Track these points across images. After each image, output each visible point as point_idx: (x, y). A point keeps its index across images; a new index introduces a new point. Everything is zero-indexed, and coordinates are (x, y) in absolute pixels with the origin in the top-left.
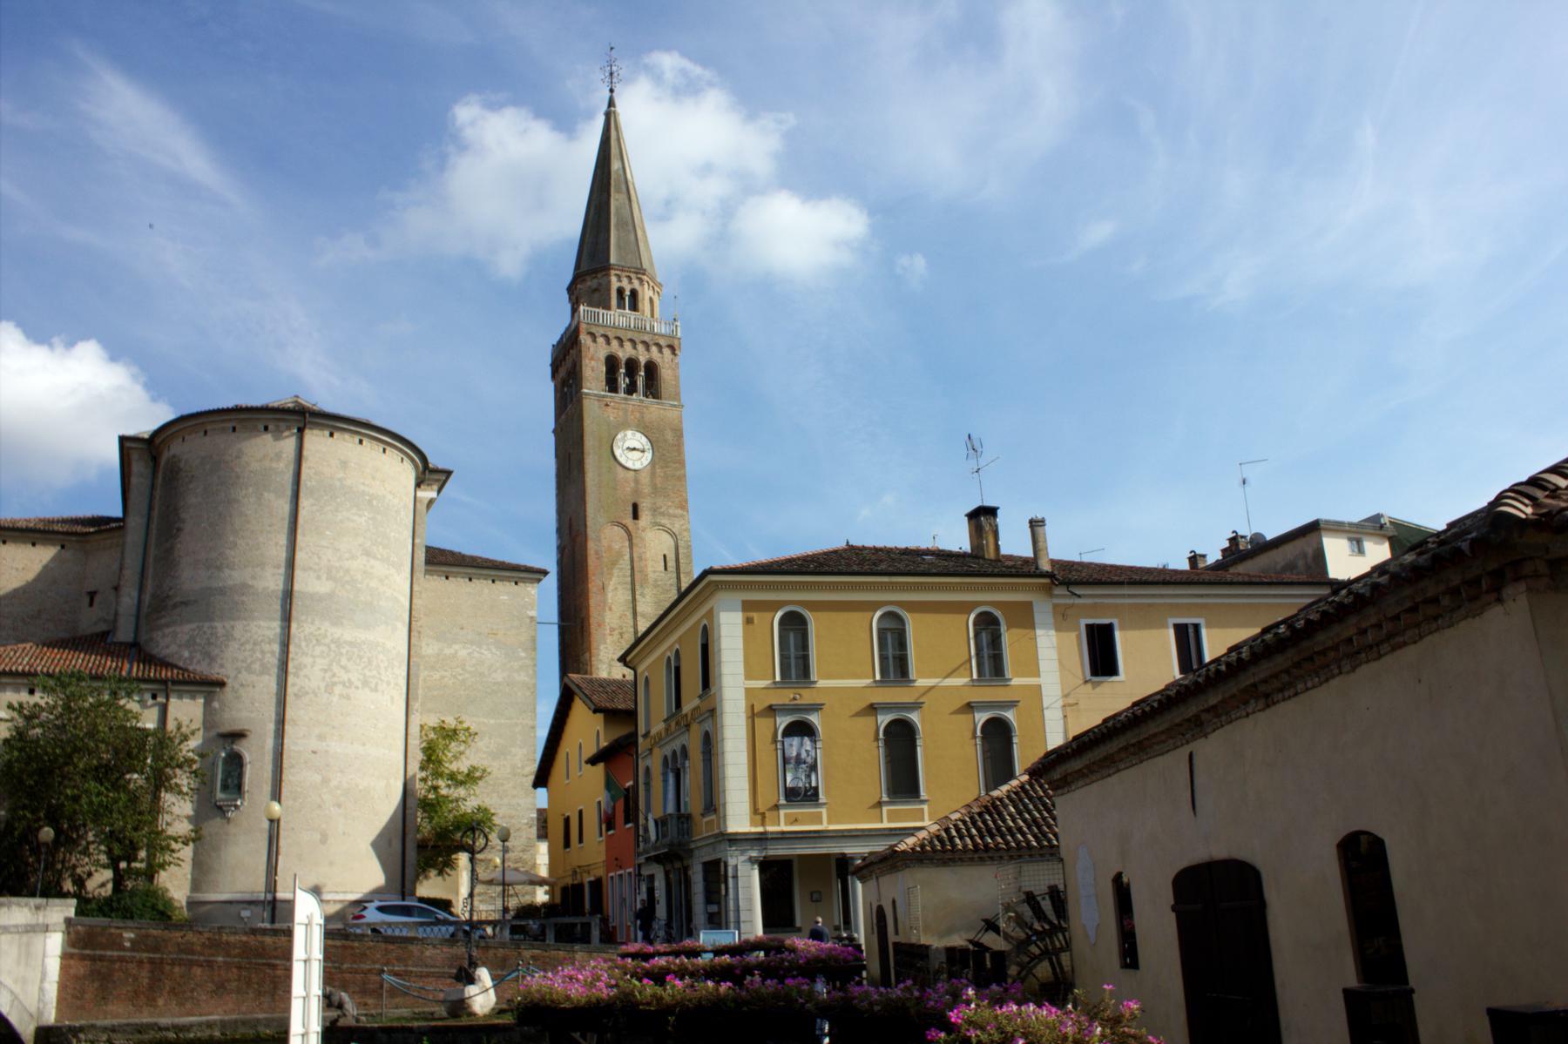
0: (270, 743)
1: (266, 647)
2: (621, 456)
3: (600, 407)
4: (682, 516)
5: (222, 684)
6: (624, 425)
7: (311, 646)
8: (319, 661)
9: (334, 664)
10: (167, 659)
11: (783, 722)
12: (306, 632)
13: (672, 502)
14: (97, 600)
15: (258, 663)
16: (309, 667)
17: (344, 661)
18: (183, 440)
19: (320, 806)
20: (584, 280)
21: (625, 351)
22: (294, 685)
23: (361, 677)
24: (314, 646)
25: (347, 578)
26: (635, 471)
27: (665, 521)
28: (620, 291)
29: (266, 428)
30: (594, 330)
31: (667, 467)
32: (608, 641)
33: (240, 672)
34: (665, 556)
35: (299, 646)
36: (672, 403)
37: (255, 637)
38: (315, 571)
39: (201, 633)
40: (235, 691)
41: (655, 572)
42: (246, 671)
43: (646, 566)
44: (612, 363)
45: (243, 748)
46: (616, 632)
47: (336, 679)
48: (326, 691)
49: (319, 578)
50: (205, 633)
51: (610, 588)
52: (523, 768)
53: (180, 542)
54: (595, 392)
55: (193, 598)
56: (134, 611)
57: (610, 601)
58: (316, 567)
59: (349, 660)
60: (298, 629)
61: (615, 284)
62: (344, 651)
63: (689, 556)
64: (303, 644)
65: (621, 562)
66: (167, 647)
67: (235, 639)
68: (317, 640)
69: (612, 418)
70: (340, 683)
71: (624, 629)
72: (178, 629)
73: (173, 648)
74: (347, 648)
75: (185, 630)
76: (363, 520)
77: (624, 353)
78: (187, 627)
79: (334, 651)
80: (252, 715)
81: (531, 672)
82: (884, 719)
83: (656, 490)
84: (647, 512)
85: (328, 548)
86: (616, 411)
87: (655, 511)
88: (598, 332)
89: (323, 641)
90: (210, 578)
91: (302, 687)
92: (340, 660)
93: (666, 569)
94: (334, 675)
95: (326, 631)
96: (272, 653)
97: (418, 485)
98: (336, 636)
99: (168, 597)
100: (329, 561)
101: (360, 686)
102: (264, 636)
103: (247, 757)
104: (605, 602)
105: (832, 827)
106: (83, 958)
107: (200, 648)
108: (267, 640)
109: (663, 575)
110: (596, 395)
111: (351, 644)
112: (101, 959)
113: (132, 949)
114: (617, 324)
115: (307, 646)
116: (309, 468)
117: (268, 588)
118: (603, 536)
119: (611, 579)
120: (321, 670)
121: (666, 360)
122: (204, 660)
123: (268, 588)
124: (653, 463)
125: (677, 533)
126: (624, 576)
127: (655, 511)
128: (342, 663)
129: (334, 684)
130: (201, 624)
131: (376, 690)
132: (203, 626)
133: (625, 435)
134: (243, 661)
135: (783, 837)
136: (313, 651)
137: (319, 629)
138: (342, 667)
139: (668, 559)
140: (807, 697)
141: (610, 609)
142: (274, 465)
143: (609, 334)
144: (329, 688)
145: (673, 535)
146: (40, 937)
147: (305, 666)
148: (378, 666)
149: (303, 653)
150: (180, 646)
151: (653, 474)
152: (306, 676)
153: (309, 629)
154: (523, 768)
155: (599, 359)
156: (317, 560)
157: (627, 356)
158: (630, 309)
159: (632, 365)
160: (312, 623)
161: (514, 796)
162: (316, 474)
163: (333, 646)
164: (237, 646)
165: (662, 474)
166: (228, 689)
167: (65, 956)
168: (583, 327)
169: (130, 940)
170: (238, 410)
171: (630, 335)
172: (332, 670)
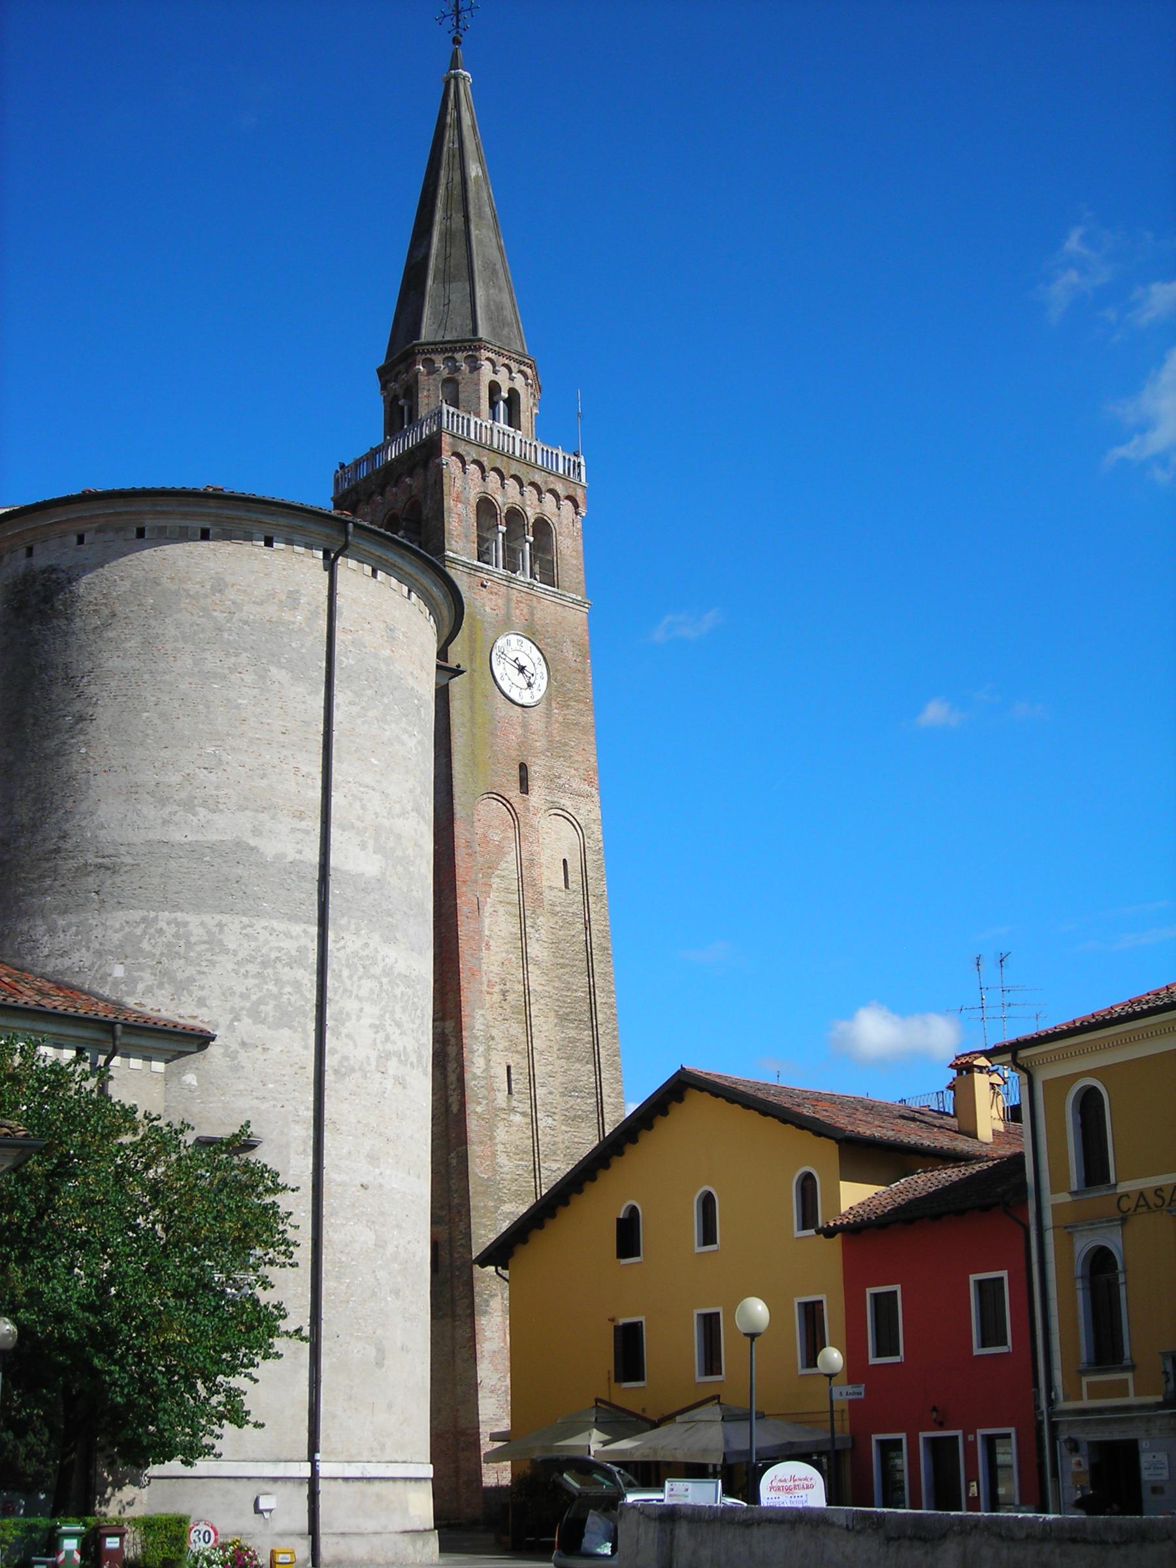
1: (286, 973)
5: (201, 1040)
6: (506, 625)
7: (355, 978)
8: (368, 1008)
9: (387, 1015)
12: (348, 950)
15: (272, 1003)
16: (354, 1017)
22: (334, 1051)
24: (360, 978)
25: (399, 853)
26: (523, 706)
27: (566, 802)
28: (494, 388)
29: (141, 533)
33: (237, 1018)
35: (339, 976)
36: (574, 596)
39: (152, 931)
40: (232, 1056)
42: (249, 1016)
44: (485, 507)
47: (389, 1047)
49: (363, 846)
50: (161, 931)
51: (487, 909)
53: (87, 744)
54: (464, 558)
57: (487, 933)
58: (358, 824)
59: (404, 1009)
62: (398, 992)
64: (346, 973)
66: (64, 954)
67: (227, 952)
68: (364, 967)
69: (487, 609)
76: (412, 743)
77: (506, 496)
80: (264, 1106)
84: (540, 783)
86: (494, 597)
88: (469, 454)
89: (372, 971)
90: (165, 822)
91: (346, 1058)
92: (393, 1012)
93: (567, 887)
94: (387, 1039)
96: (297, 985)
100: (376, 813)
102: (280, 949)
104: (479, 932)
117: (284, 856)
121: (565, 522)
122: (161, 986)
124: (548, 697)
126: (507, 890)
127: (552, 780)
128: (397, 1016)
129: (388, 1055)
130: (152, 914)
133: (508, 643)
134: (242, 996)
136: (359, 987)
138: (399, 1025)
141: (488, 949)
142: (287, 616)
143: (485, 461)
149: (345, 991)
150: (99, 954)
151: (548, 714)
152: (348, 1036)
156: (361, 812)
159: (515, 516)
160: (357, 933)
163: (385, 980)
164: (230, 966)
165: (561, 719)
170: (87, 497)
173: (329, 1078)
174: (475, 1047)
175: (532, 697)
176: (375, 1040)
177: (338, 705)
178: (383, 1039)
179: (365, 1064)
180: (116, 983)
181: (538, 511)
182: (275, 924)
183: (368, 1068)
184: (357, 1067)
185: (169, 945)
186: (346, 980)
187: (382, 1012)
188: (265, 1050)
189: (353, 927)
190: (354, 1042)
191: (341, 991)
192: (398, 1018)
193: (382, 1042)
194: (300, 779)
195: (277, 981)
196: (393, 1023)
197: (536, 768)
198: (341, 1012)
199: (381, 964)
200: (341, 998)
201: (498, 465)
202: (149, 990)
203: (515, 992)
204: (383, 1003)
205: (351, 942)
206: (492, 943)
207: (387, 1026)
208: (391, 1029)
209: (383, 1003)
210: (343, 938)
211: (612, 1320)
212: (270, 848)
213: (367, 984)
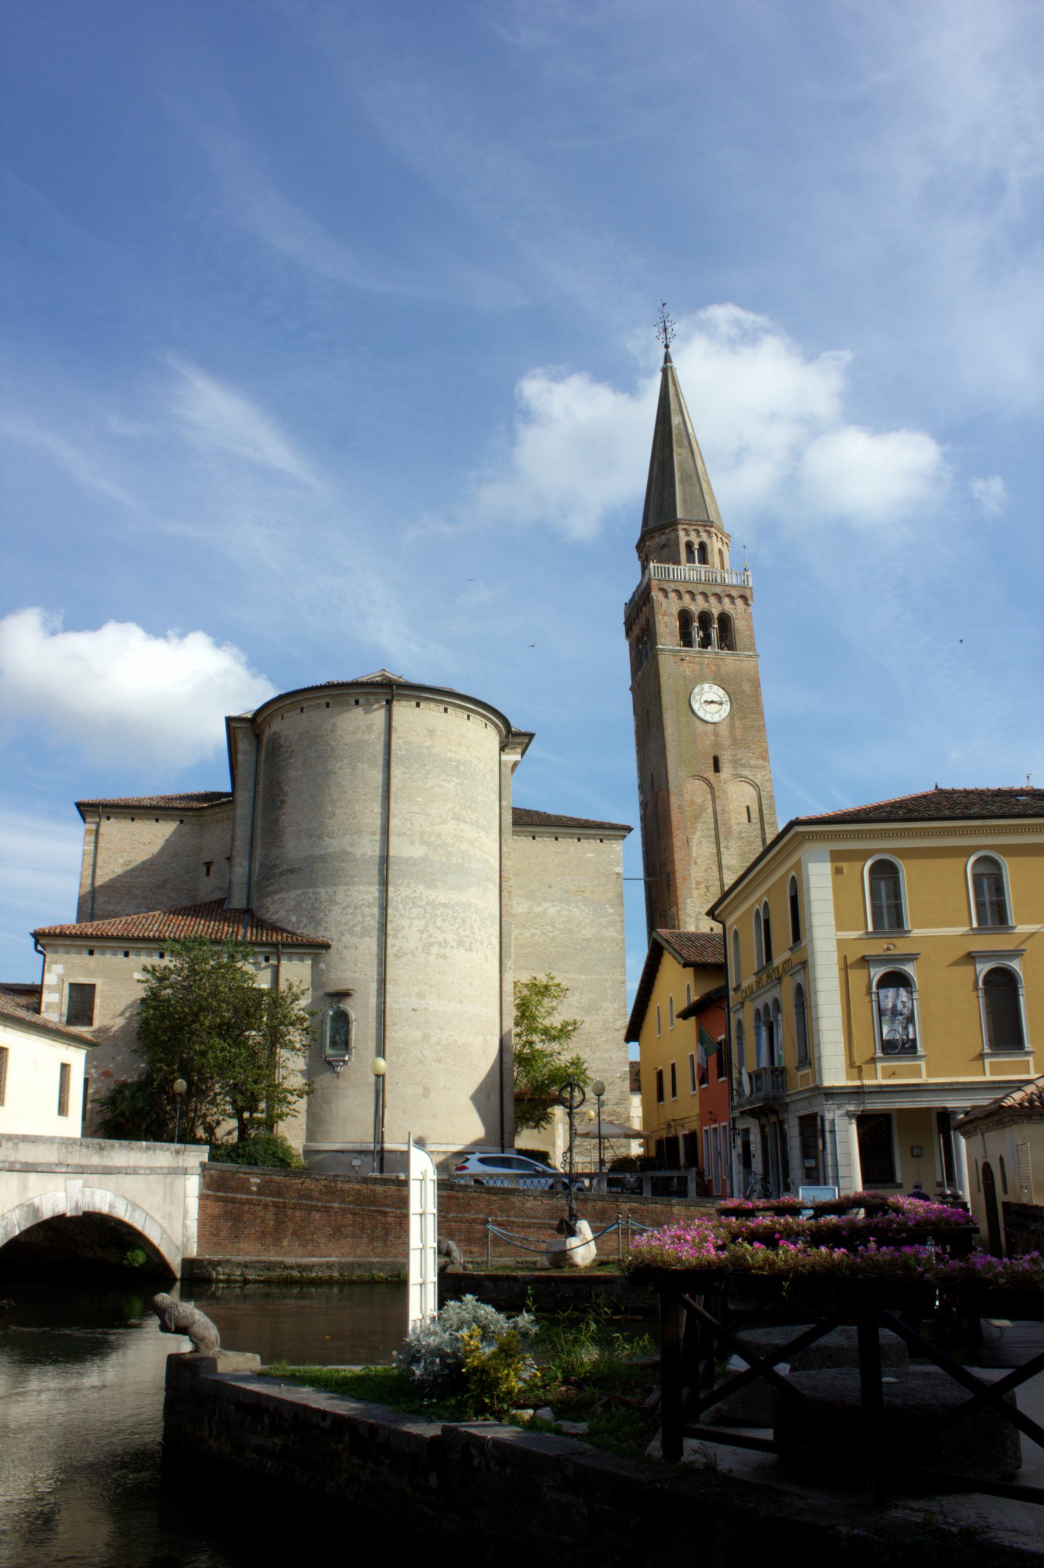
0: (373, 1001)
1: (367, 911)
2: (699, 710)
3: (676, 663)
4: (763, 767)
5: (327, 946)
6: (701, 679)
7: (407, 908)
8: (415, 922)
9: (430, 925)
10: (277, 924)
11: (877, 973)
12: (402, 896)
13: (753, 753)
14: (213, 869)
17: (439, 923)
18: (282, 719)
19: (421, 1062)
20: (653, 537)
21: (697, 605)
22: (393, 946)
23: (456, 937)
24: (410, 908)
25: (439, 842)
26: (714, 723)
27: (745, 773)
28: (689, 545)
30: (665, 586)
31: (746, 718)
32: (695, 895)
33: (343, 935)
34: (748, 808)
35: (396, 909)
36: (747, 653)
37: (356, 901)
38: (408, 837)
41: (738, 824)
43: (729, 818)
44: (685, 617)
45: (347, 1006)
46: (702, 885)
47: (432, 940)
48: (423, 951)
49: (412, 843)
50: (310, 898)
51: (695, 842)
52: (614, 1022)
54: (670, 647)
55: (297, 866)
56: (245, 880)
57: (695, 855)
58: (409, 833)
59: (444, 921)
60: (395, 892)
61: (683, 539)
62: (439, 912)
63: (772, 807)
64: (401, 907)
65: (704, 815)
66: (277, 912)
67: (338, 904)
68: (413, 903)
69: (688, 673)
70: (436, 943)
71: (710, 882)
72: (286, 895)
73: (282, 914)
74: (442, 910)
75: (291, 897)
76: (451, 785)
77: (696, 607)
78: (293, 894)
79: (430, 913)
80: (356, 975)
81: (619, 928)
82: (983, 968)
83: (735, 742)
85: (419, 813)
87: (736, 762)
88: (669, 587)
89: (418, 903)
90: (312, 846)
91: (401, 948)
92: (435, 922)
93: (749, 821)
94: (430, 936)
95: (421, 893)
96: (372, 915)
97: (502, 749)
98: (431, 898)
99: (275, 865)
100: (421, 826)
101: (455, 945)
102: (364, 900)
103: (353, 1015)
104: (689, 855)
105: (931, 1080)
106: (218, 1199)
107: (306, 913)
108: (367, 904)
109: (747, 826)
110: (670, 651)
111: (445, 905)
112: (233, 1201)
113: (258, 1193)
114: (687, 578)
115: (404, 908)
116: (399, 738)
118: (684, 792)
119: (694, 833)
120: (418, 931)
121: (739, 611)
122: (310, 924)
123: (366, 854)
124: (731, 715)
125: (759, 784)
127: (736, 763)
129: (431, 944)
131: (470, 949)
132: (308, 892)
133: (702, 689)
134: (345, 924)
135: (881, 1091)
136: (410, 913)
137: (415, 892)
138: (439, 928)
139: (751, 810)
140: (901, 947)
141: (695, 863)
142: (366, 737)
143: (682, 589)
144: (427, 948)
145: (755, 786)
146: (181, 1178)
147: (403, 928)
148: (472, 926)
150: (287, 911)
151: (732, 726)
152: (404, 937)
153: (404, 892)
154: (614, 1022)
155: (672, 615)
156: (410, 826)
157: (700, 609)
158: (699, 563)
160: (408, 886)
161: (606, 1051)
162: (405, 743)
163: (428, 908)
164: (339, 911)
165: (741, 726)
166: (332, 951)
167: (202, 1197)
168: (654, 583)
169: (257, 1185)
170: (330, 686)
171: (701, 588)
172: (428, 931)
174: (687, 920)
175: (720, 717)
177: (395, 776)
180: (293, 924)
181: (720, 609)
182: (361, 888)
185: (313, 904)
188: (356, 948)
194: (374, 816)
195: (364, 916)
197: (725, 757)
198: (398, 926)
201: (690, 589)
202: (305, 926)
203: (714, 885)
206: (699, 861)
211: (656, 1069)
212: (358, 851)
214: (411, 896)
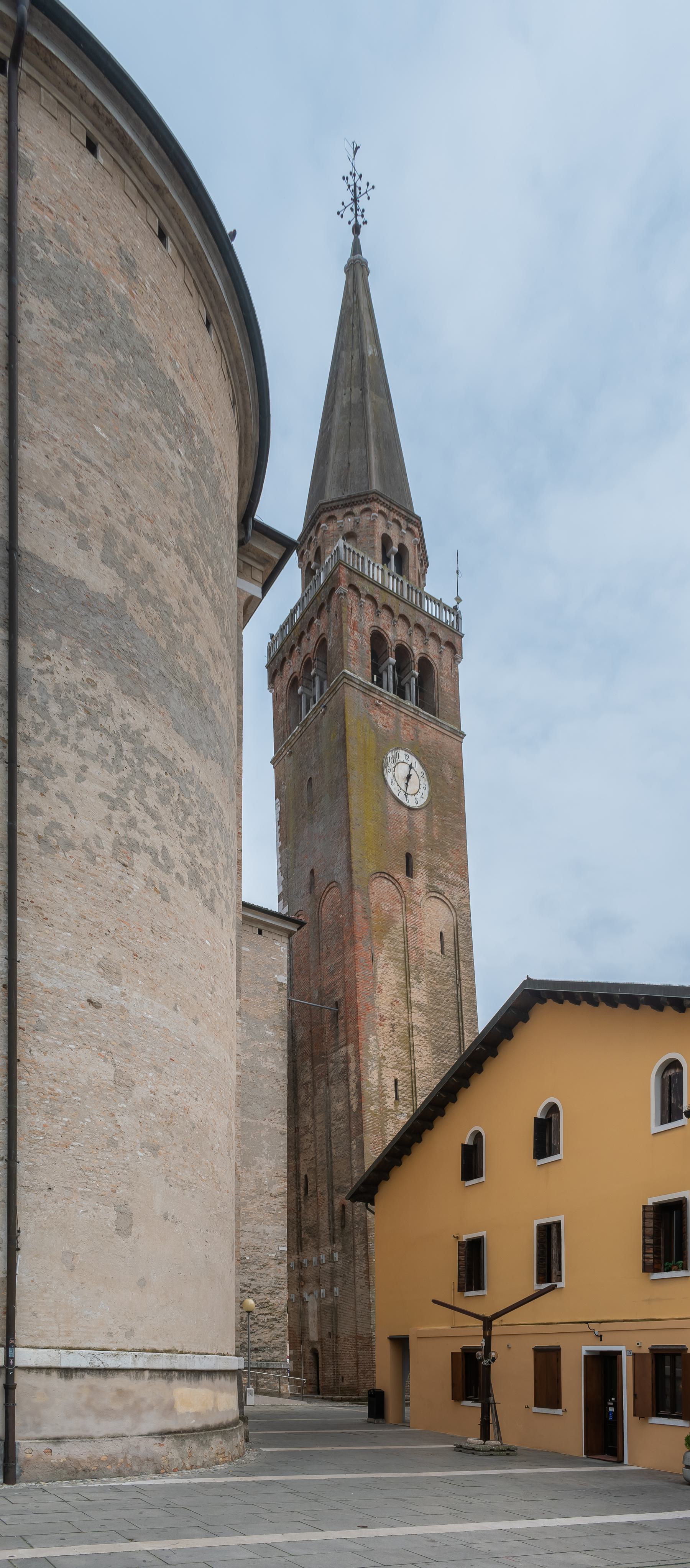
7: (72, 721)
8: (94, 769)
9: (131, 794)
24: (81, 724)
64: (54, 709)
91: (60, 827)
92: (141, 794)
94: (132, 823)
95: (108, 696)
136: (80, 737)
149: (54, 733)
152: (61, 796)
163: (126, 745)
173: (26, 846)
176: (109, 818)
178: (124, 821)
179: (93, 845)
183: (97, 851)
184: (78, 843)
186: (55, 719)
187: (122, 786)
189: (65, 648)
190: (72, 808)
191: (46, 730)
192: (151, 805)
193: (122, 824)
196: (141, 807)
199: (120, 721)
200: (48, 739)
204: (124, 774)
205: (63, 669)
207: (132, 807)
208: (140, 815)
209: (124, 774)
210: (48, 658)
213: (91, 740)
214: (81, 690)
